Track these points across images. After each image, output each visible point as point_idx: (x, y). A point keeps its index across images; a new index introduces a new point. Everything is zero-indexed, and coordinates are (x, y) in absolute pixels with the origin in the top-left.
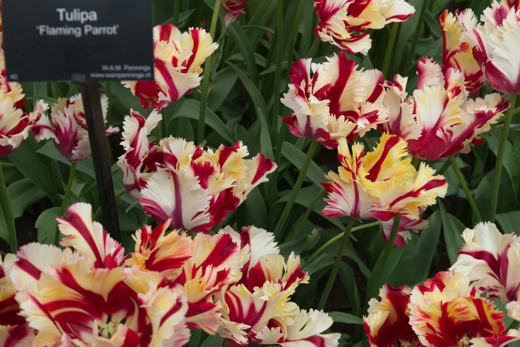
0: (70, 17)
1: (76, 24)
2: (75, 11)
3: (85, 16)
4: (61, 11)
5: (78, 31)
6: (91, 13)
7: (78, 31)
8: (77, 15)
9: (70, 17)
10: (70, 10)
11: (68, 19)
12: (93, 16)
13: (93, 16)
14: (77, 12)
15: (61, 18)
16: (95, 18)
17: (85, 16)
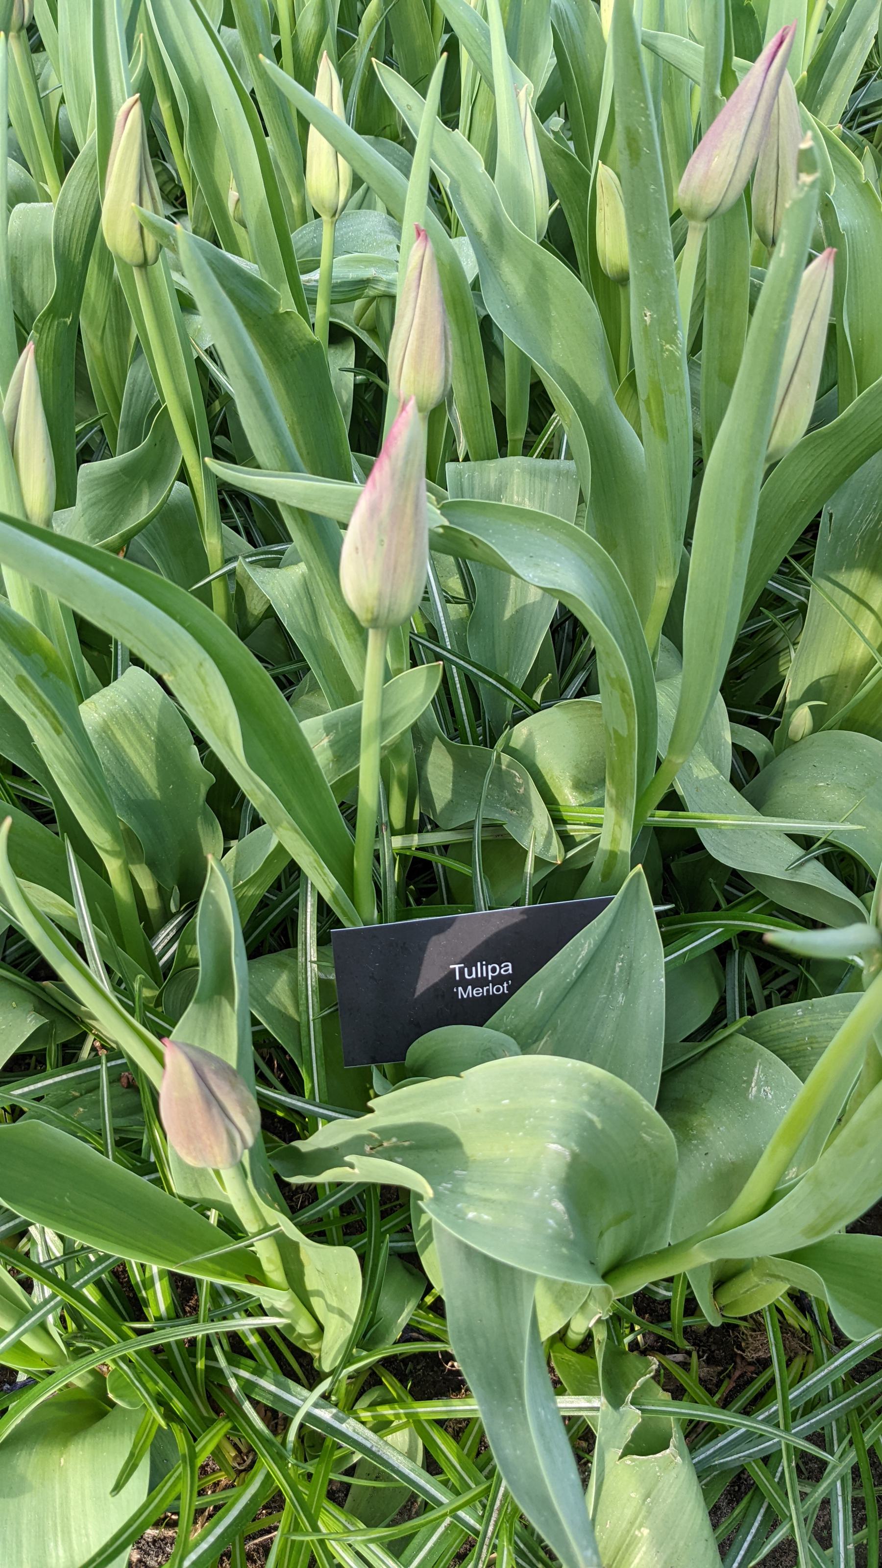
0: (470, 974)
1: (481, 982)
2: (479, 964)
4: (457, 967)
9: (470, 974)
11: (467, 977)
12: (508, 968)
14: (482, 966)
15: (458, 978)
16: (510, 971)
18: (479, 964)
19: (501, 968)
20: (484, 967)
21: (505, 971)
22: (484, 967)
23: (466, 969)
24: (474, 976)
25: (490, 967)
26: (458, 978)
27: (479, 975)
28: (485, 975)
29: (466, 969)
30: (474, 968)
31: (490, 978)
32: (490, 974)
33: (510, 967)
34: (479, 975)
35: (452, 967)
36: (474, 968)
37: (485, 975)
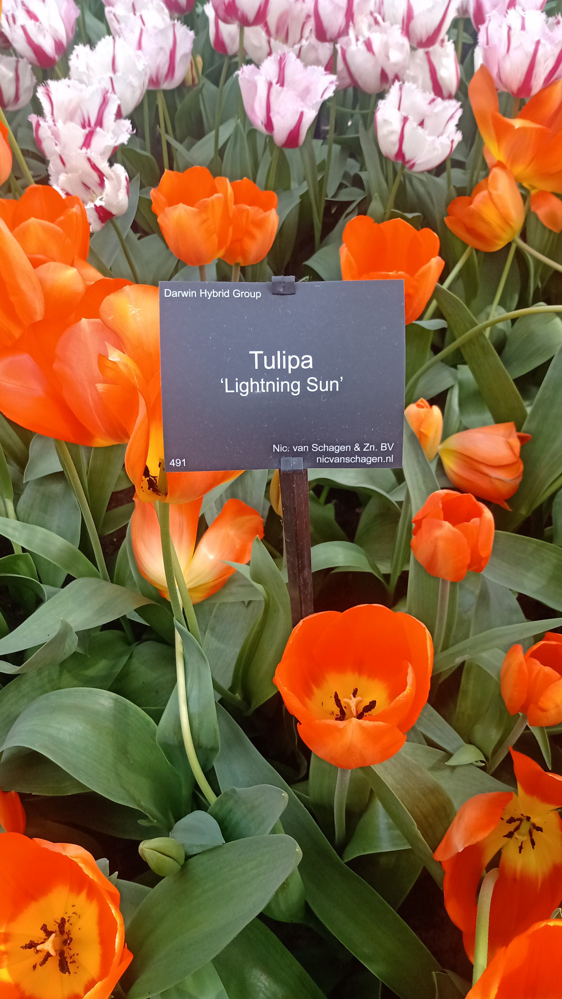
0: (269, 364)
1: (280, 374)
2: (279, 352)
3: (294, 362)
4: (256, 353)
5: (295, 386)
6: (303, 358)
7: (295, 386)
8: (282, 361)
9: (269, 364)
10: (270, 353)
12: (308, 362)
13: (308, 362)
14: (282, 355)
15: (256, 367)
16: (311, 366)
17: (294, 362)
18: (279, 352)
19: (301, 361)
20: (284, 357)
21: (306, 365)
22: (284, 357)
23: (265, 357)
24: (273, 366)
25: (290, 358)
26: (256, 367)
27: (279, 367)
28: (284, 367)
29: (265, 357)
30: (273, 357)
31: (290, 372)
32: (290, 367)
33: (311, 361)
34: (279, 367)
35: (251, 352)
36: (273, 357)
37: (284, 367)
